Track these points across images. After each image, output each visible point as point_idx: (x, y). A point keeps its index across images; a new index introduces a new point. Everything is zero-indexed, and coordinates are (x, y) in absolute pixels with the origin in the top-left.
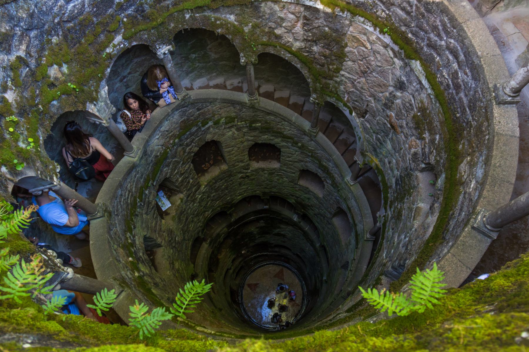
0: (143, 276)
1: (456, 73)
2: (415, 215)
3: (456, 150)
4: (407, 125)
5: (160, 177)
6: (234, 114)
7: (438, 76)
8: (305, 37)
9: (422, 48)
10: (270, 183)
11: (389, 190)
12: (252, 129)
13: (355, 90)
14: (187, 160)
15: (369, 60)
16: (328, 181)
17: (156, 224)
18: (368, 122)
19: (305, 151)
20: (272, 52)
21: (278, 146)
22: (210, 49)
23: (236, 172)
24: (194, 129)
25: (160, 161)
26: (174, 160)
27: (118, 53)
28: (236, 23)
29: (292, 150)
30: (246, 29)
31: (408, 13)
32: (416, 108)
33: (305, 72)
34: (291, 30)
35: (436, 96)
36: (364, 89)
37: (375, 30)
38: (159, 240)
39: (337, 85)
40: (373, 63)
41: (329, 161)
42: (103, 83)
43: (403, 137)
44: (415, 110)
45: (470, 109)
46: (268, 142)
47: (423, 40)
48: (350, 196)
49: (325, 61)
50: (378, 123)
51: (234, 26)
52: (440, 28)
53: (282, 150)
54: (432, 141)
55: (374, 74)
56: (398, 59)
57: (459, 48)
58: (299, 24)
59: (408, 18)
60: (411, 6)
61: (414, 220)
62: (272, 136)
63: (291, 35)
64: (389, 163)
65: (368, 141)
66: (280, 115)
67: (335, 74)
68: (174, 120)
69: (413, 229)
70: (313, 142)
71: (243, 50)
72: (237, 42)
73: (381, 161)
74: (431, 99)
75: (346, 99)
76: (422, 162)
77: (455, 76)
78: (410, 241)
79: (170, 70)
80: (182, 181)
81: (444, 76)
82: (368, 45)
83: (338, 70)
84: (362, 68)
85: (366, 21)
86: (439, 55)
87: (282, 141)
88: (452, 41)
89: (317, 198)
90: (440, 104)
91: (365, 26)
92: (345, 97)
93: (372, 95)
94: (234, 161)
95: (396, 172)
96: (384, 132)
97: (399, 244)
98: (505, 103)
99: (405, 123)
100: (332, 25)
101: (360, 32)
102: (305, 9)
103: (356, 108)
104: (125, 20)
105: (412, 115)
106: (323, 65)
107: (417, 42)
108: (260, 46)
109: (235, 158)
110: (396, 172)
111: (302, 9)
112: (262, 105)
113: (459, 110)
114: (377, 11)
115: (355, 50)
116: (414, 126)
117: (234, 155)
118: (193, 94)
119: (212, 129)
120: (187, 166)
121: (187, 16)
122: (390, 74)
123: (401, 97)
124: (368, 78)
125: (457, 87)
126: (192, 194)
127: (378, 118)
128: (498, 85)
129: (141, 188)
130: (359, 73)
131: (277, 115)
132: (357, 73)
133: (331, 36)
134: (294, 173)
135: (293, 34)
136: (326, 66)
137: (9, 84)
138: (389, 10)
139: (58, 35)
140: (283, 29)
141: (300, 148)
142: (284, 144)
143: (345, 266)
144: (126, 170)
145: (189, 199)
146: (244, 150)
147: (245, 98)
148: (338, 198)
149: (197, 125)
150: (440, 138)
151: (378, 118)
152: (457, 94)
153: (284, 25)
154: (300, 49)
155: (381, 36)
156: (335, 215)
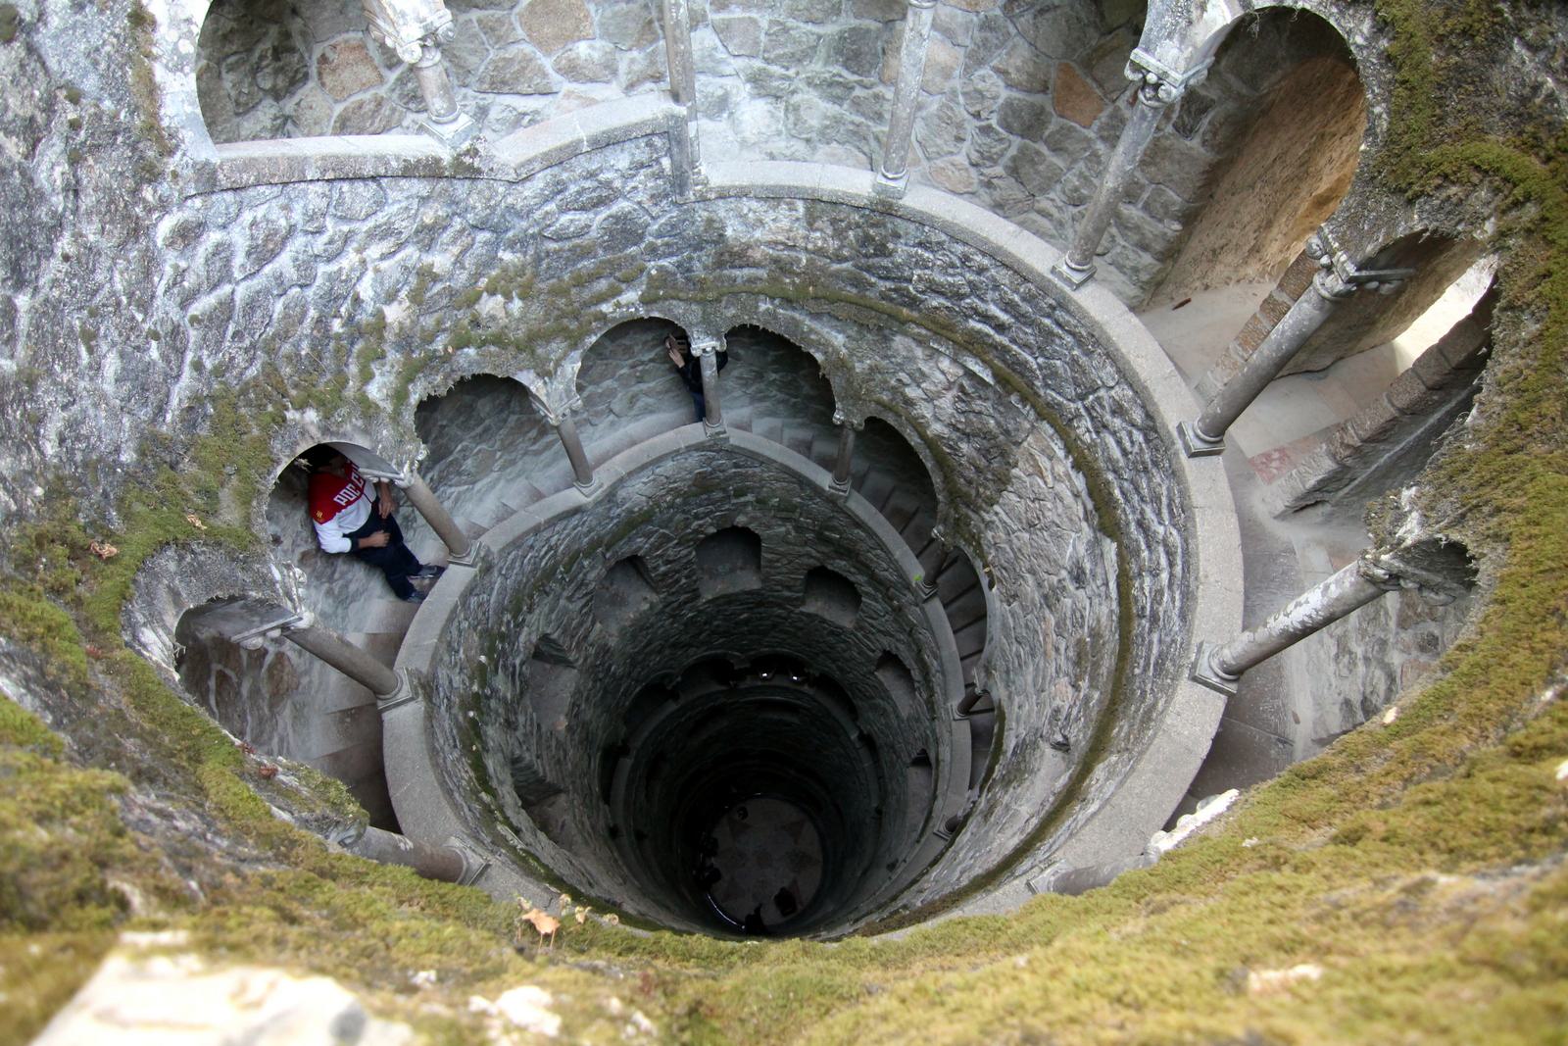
0: (488, 698)
5: (625, 549)
9: (1128, 524)
17: (581, 624)
24: (717, 495)
25: (634, 522)
30: (859, 368)
31: (1125, 453)
33: (937, 480)
38: (572, 656)
41: (936, 657)
42: (577, 354)
48: (946, 735)
52: (1164, 500)
54: (1087, 699)
58: (949, 396)
59: (1122, 463)
71: (842, 400)
72: (837, 383)
80: (665, 574)
82: (1050, 479)
83: (991, 502)
86: (1149, 547)
101: (1043, 452)
106: (969, 482)
118: (736, 438)
129: (578, 552)
133: (995, 438)
137: (403, 294)
139: (525, 254)
142: (869, 589)
143: (892, 867)
147: (825, 480)
149: (724, 490)
154: (940, 437)
155: (1073, 473)
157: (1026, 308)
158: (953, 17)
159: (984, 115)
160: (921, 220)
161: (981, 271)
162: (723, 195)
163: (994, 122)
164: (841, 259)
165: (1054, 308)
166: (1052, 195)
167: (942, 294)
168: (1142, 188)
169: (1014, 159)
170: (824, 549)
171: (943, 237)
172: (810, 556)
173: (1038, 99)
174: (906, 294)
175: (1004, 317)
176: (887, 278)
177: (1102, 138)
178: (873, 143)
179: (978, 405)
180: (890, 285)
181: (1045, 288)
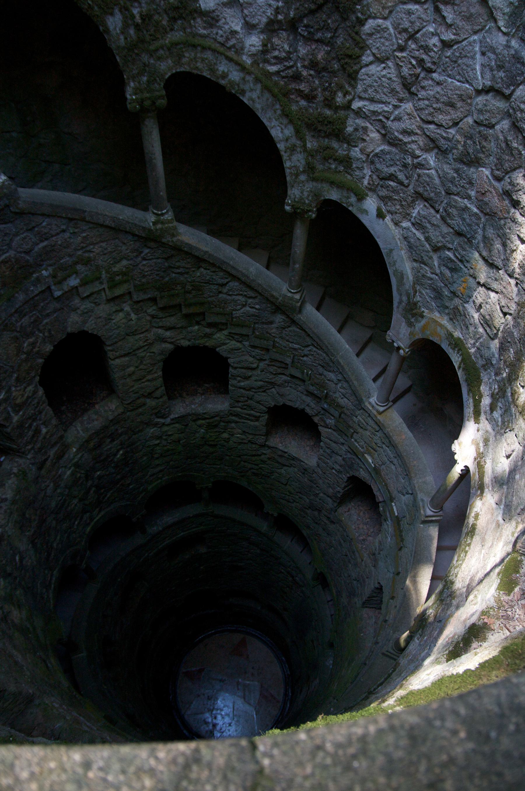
21: (222, 350)
29: (251, 359)
55: (434, 75)
70: (294, 328)
80: (21, 425)
84: (405, 71)
89: (305, 471)
103: (390, 198)
115: (388, 24)
117: (134, 377)
132: (393, 91)
134: (257, 419)
145: (43, 472)
146: (154, 365)
156: (343, 500)
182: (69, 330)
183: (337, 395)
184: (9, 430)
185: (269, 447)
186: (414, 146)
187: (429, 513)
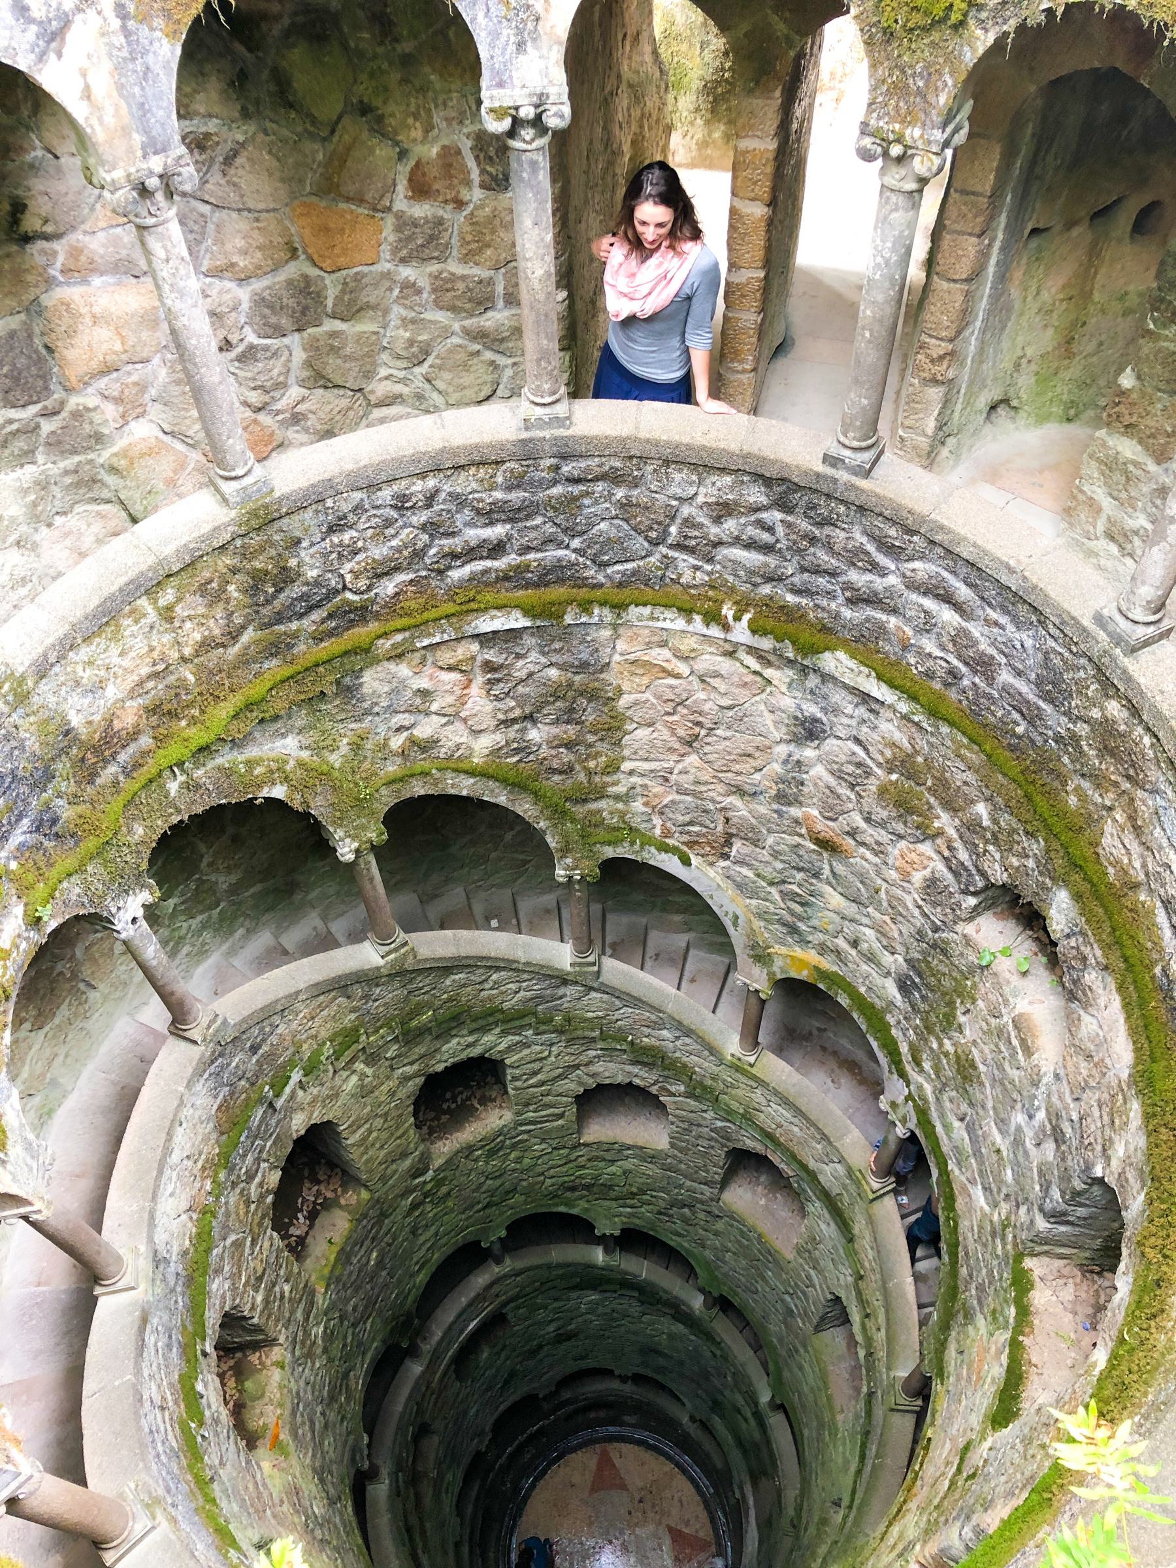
1: (963, 632)
2: (1023, 1042)
3: (1063, 814)
4: (868, 820)
5: (212, 1318)
6: (353, 1016)
7: (912, 661)
8: (501, 716)
9: (837, 616)
10: (498, 1182)
11: (888, 1017)
12: (409, 1037)
13: (678, 797)
14: (260, 1224)
15: (695, 702)
16: (673, 1089)
18: (743, 863)
19: (580, 1033)
20: (422, 792)
21: (493, 1054)
22: (210, 865)
23: (397, 1196)
26: (229, 1242)
27: (17, 972)
28: (305, 754)
29: (538, 1048)
30: (335, 759)
31: (767, 549)
32: (879, 765)
33: (525, 808)
34: (457, 714)
35: (933, 713)
36: (706, 783)
37: (689, 621)
39: (620, 806)
40: (707, 707)
41: (658, 1025)
43: (868, 855)
44: (879, 772)
45: (1051, 702)
46: (463, 1056)
47: (830, 595)
48: (758, 1096)
49: (572, 757)
50: (776, 854)
51: (301, 764)
52: (871, 548)
53: (508, 1062)
54: (972, 827)
55: (718, 732)
56: (778, 668)
57: (945, 574)
58: (476, 689)
59: (772, 561)
60: (770, 529)
61: (1028, 1051)
62: (471, 1033)
63: (459, 725)
64: (855, 944)
65: (761, 915)
66: (482, 958)
67: (607, 779)
68: (199, 1113)
69: (1048, 1079)
70: (593, 994)
71: (339, 822)
72: (319, 807)
73: (823, 949)
74: (917, 724)
75: (658, 831)
76: (965, 892)
77: (960, 641)
78: (1055, 1116)
79: (154, 963)
80: (267, 1302)
81: (930, 655)
82: (683, 668)
83: (612, 768)
84: (681, 732)
85: (658, 611)
86: (894, 611)
87: (505, 1033)
88: (917, 565)
90: (952, 724)
91: (660, 624)
92: (654, 827)
93: (739, 791)
94: (380, 1164)
95: (887, 959)
96: (800, 870)
97: (1018, 1143)
98: (1147, 643)
99: (858, 820)
100: (566, 658)
101: (649, 645)
102: (482, 644)
103: (696, 842)
104: (13, 865)
105: (874, 789)
106: (568, 770)
107: (816, 606)
108: (384, 791)
109: (383, 1153)
110: (887, 959)
111: (475, 647)
112: (424, 952)
113: (1016, 715)
114: (680, 575)
116: (894, 814)
119: (300, 1093)
120: (266, 1244)
121: (173, 787)
122: (766, 713)
123: (819, 759)
124: (707, 749)
125: (983, 666)
126: (300, 1333)
127: (770, 840)
128: (1105, 612)
130: (677, 746)
131: (471, 962)
132: (672, 750)
133: (570, 684)
135: (465, 720)
136: (578, 767)
138: (710, 560)
140: (434, 717)
141: (560, 1031)
144: (127, 1339)
145: (297, 1353)
146: (400, 1116)
147: (369, 955)
148: (719, 1124)
150: (995, 808)
151: (770, 840)
152: (990, 680)
153: (434, 707)
154: (495, 752)
157: (516, 496)
158: (116, 242)
159: (234, 338)
160: (315, 497)
161: (430, 499)
162: (42, 670)
163: (252, 338)
164: (233, 635)
165: (557, 468)
166: (383, 372)
167: (397, 569)
168: (490, 282)
169: (308, 364)
170: (420, 1050)
171: (358, 496)
172: (406, 1078)
173: (292, 270)
174: (352, 608)
175: (498, 531)
176: (311, 609)
177: (403, 261)
178: (111, 480)
179: (521, 669)
180: (316, 616)
181: (528, 452)
182: (295, 1136)
183: (678, 1055)
184: (255, 1320)
185: (586, 1145)
186: (711, 794)
187: (876, 1186)
